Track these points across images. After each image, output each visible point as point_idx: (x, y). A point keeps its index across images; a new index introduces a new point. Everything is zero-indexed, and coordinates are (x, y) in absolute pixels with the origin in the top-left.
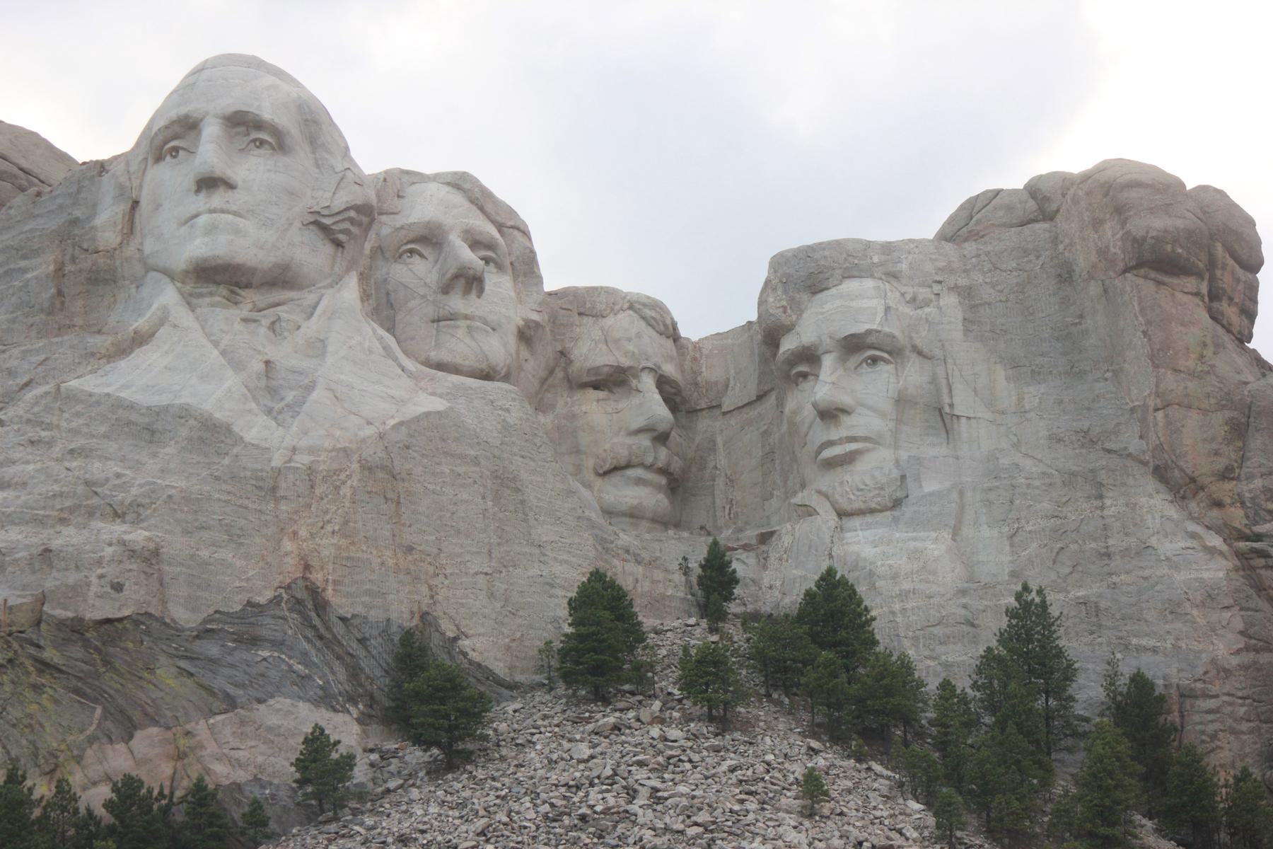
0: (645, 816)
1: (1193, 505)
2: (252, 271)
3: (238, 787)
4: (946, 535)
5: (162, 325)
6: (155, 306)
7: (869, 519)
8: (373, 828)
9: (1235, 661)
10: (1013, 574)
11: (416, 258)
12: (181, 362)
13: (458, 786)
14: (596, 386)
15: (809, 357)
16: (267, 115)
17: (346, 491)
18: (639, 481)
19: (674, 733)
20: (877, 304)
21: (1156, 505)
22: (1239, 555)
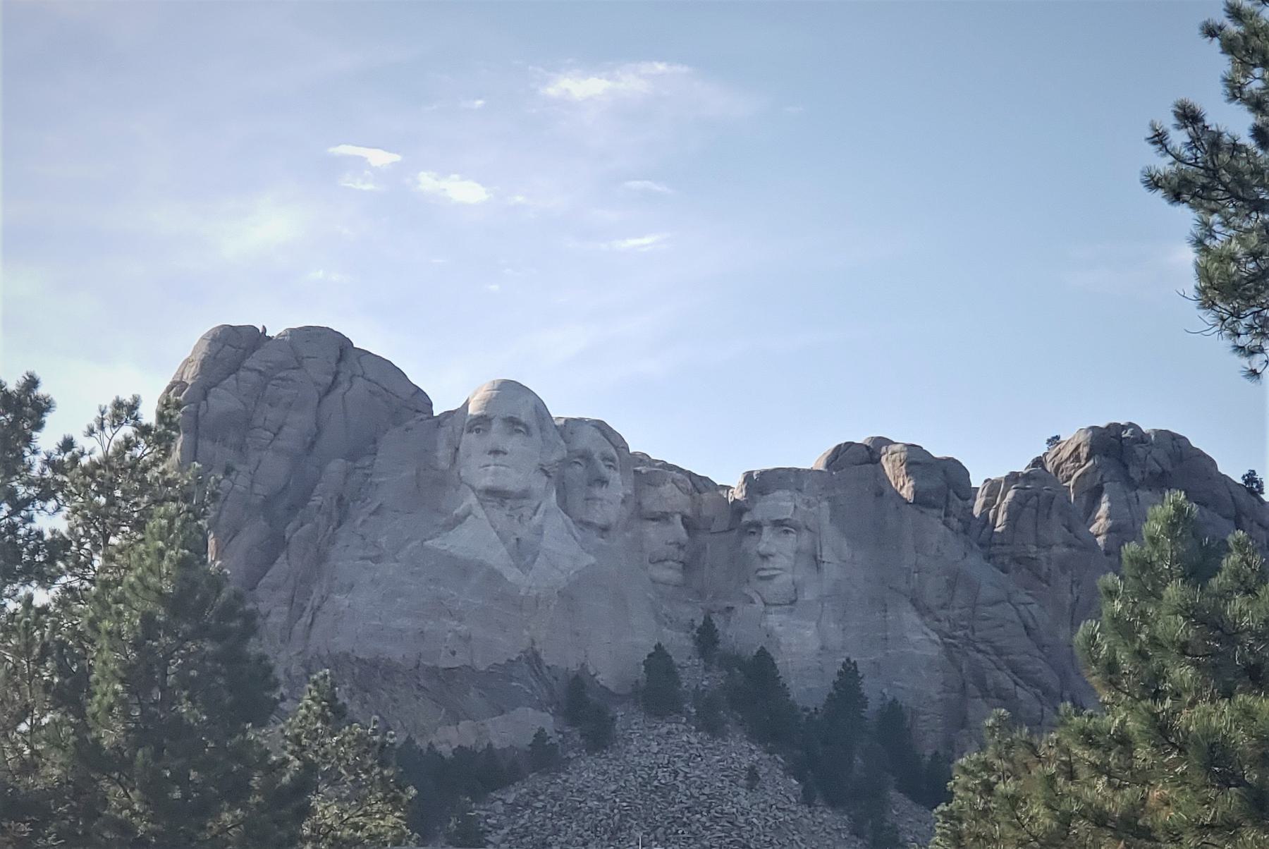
0: (682, 787)
1: (927, 619)
2: (512, 493)
3: (504, 750)
4: (814, 624)
5: (469, 514)
6: (465, 504)
7: (778, 608)
8: (565, 781)
9: (938, 697)
10: (843, 648)
11: (578, 467)
12: (476, 538)
13: (601, 761)
14: (653, 520)
15: (758, 526)
16: (523, 419)
17: (552, 607)
18: (670, 568)
19: (693, 740)
20: (790, 504)
21: (910, 617)
22: (945, 643)
